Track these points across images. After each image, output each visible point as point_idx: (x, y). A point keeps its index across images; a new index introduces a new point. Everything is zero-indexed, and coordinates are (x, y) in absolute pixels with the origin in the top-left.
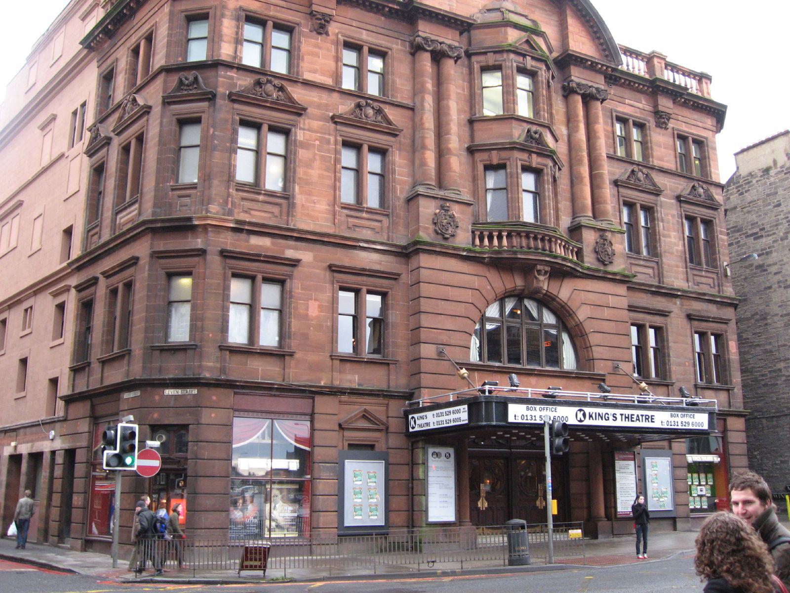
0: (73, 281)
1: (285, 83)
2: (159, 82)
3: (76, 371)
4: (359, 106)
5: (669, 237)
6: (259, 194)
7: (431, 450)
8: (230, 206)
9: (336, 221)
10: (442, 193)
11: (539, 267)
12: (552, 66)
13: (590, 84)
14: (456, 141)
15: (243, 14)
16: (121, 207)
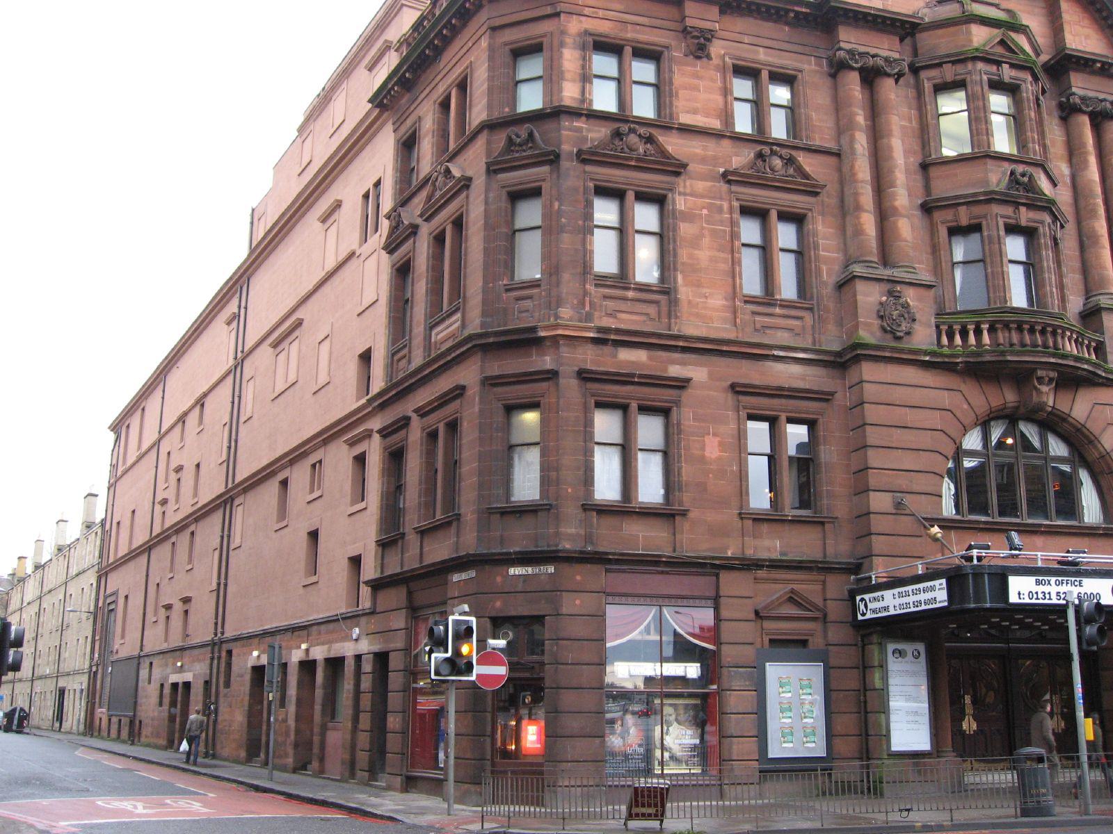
0: (376, 424)
1: (654, 132)
2: (480, 144)
3: (385, 545)
4: (760, 156)
6: (628, 289)
7: (891, 647)
8: (587, 308)
9: (738, 320)
10: (886, 273)
11: (1040, 373)
12: (1041, 75)
13: (1101, 96)
14: (903, 196)
15: (590, 39)
16: (436, 317)
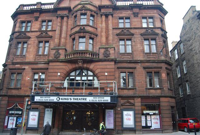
5: (137, 46)
7: (46, 109)
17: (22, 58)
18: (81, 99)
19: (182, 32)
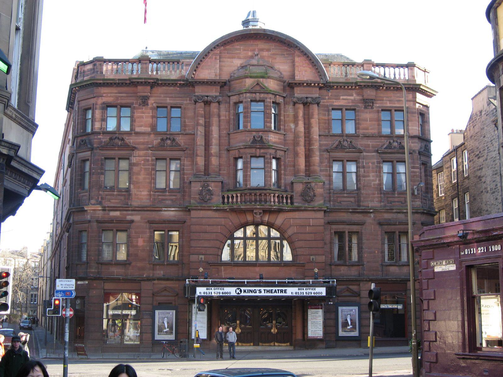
4: (162, 140)
5: (369, 176)
8: (100, 200)
17: (122, 195)
18: (277, 291)
19: (468, 129)
